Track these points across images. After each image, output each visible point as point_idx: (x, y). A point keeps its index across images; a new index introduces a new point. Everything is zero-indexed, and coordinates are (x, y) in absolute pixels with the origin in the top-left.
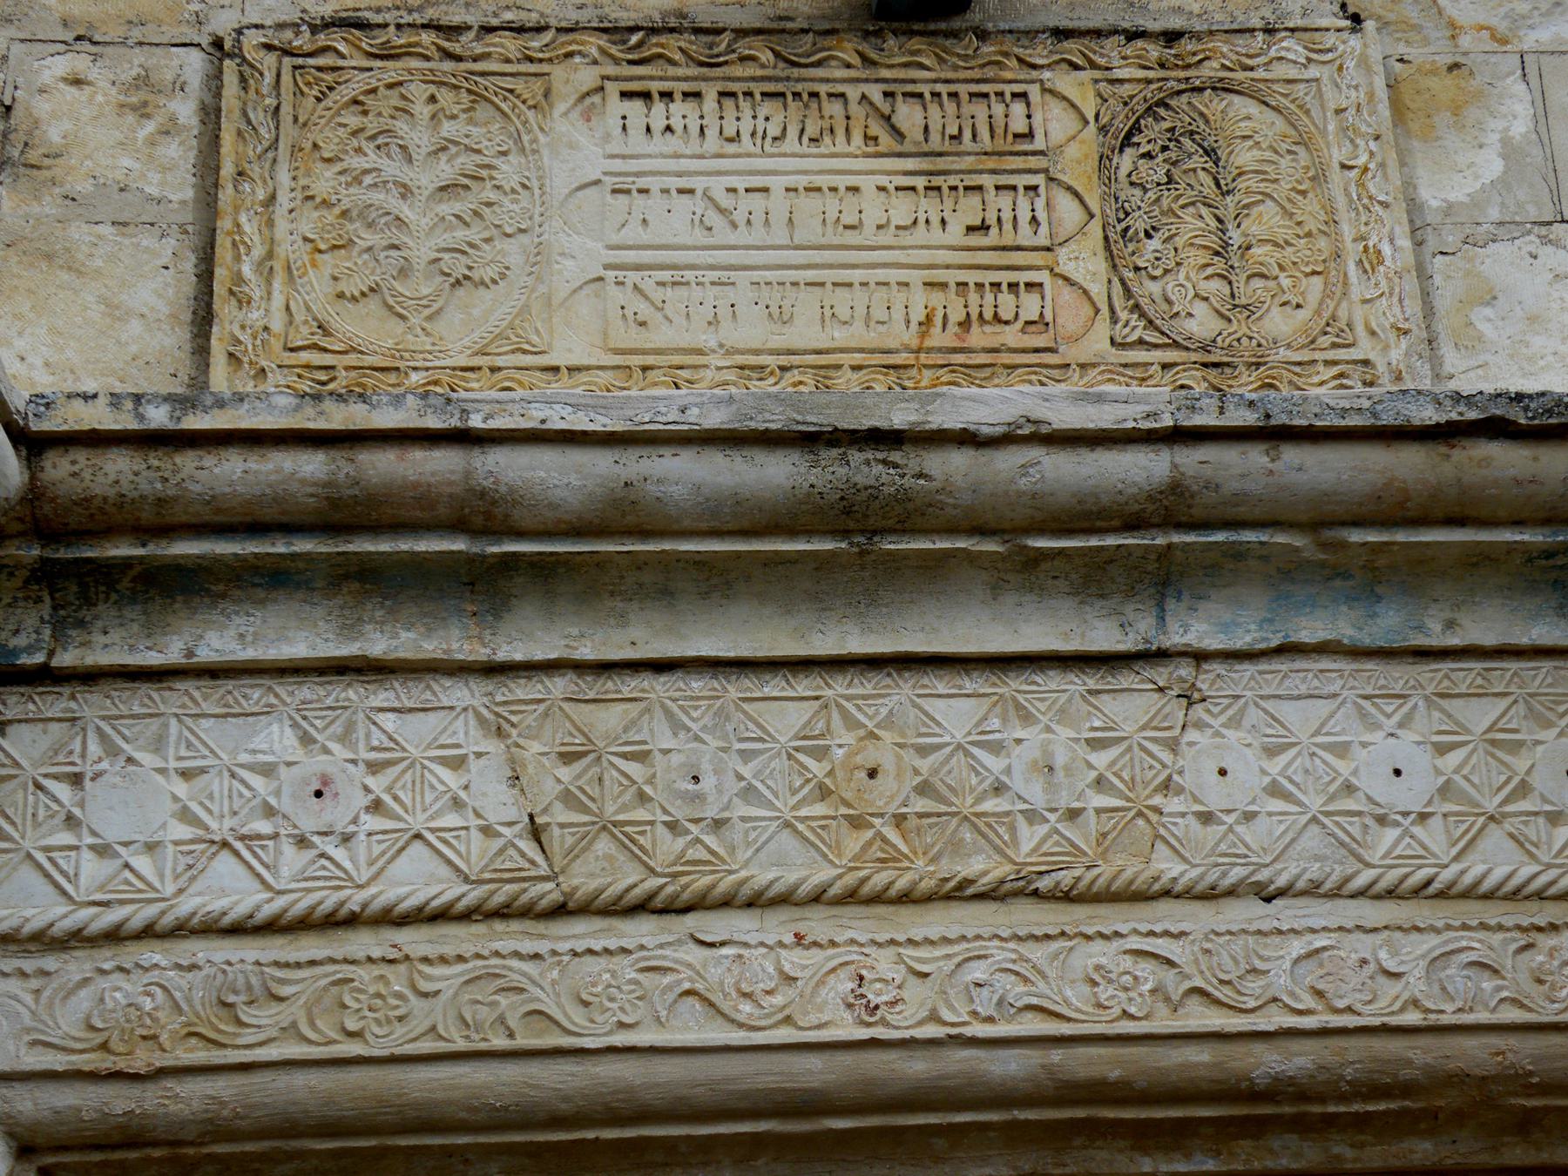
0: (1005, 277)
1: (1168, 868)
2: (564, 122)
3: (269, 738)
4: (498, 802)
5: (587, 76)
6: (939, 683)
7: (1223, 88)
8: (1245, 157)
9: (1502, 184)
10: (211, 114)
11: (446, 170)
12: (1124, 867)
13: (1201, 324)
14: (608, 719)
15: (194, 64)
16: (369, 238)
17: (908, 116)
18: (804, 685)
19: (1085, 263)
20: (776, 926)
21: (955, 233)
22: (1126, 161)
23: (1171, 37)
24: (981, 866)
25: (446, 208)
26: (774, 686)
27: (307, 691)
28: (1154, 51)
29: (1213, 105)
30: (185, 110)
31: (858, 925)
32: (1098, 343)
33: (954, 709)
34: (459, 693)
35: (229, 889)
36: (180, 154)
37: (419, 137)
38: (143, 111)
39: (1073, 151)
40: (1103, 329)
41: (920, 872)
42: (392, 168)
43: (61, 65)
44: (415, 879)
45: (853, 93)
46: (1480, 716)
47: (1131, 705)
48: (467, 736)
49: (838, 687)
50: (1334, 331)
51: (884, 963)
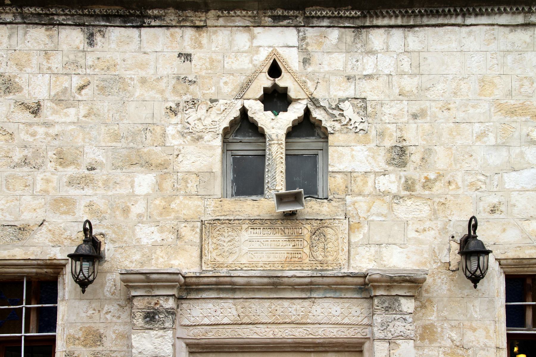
0: (296, 252)
1: (309, 321)
2: (243, 232)
3: (210, 306)
4: (235, 313)
5: (246, 226)
6: (285, 300)
7: (327, 227)
8: (329, 236)
9: (362, 239)
10: (201, 230)
11: (229, 239)
12: (304, 321)
13: (320, 258)
14: (247, 304)
15: (199, 224)
16: (221, 248)
17: (286, 231)
18: (269, 301)
19: (307, 250)
20: (265, 326)
21: (291, 246)
22: (314, 237)
23: (321, 220)
24: (287, 320)
25: (229, 244)
26: (266, 301)
27: (214, 300)
28: (319, 222)
29: (325, 229)
30: (198, 230)
31: (274, 326)
32: (307, 261)
33: (286, 303)
34: (230, 301)
35: (206, 321)
36: (198, 236)
37: (226, 235)
38: (193, 230)
39: (307, 236)
40: (308, 259)
41: (281, 321)
42: (223, 238)
43: (184, 225)
44: (226, 321)
45: (280, 228)
46: (347, 305)
47: (306, 303)
48: (231, 305)
49: (273, 301)
50: (336, 259)
51: (277, 330)
